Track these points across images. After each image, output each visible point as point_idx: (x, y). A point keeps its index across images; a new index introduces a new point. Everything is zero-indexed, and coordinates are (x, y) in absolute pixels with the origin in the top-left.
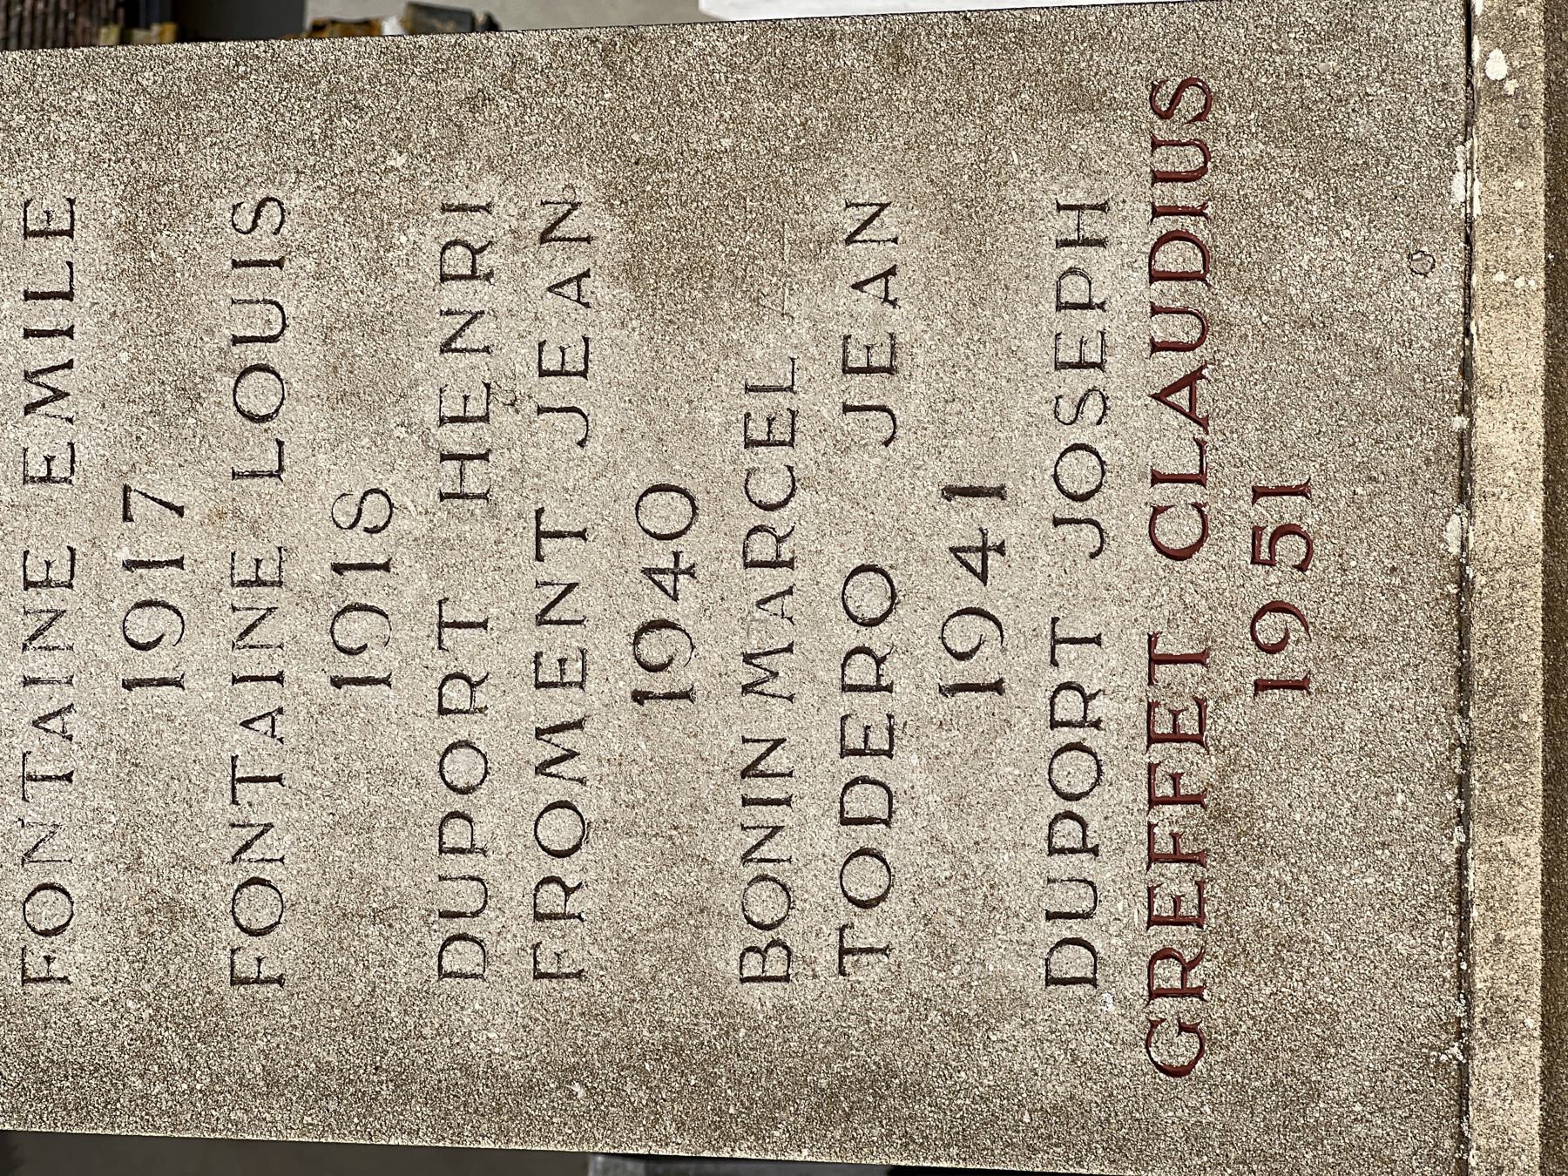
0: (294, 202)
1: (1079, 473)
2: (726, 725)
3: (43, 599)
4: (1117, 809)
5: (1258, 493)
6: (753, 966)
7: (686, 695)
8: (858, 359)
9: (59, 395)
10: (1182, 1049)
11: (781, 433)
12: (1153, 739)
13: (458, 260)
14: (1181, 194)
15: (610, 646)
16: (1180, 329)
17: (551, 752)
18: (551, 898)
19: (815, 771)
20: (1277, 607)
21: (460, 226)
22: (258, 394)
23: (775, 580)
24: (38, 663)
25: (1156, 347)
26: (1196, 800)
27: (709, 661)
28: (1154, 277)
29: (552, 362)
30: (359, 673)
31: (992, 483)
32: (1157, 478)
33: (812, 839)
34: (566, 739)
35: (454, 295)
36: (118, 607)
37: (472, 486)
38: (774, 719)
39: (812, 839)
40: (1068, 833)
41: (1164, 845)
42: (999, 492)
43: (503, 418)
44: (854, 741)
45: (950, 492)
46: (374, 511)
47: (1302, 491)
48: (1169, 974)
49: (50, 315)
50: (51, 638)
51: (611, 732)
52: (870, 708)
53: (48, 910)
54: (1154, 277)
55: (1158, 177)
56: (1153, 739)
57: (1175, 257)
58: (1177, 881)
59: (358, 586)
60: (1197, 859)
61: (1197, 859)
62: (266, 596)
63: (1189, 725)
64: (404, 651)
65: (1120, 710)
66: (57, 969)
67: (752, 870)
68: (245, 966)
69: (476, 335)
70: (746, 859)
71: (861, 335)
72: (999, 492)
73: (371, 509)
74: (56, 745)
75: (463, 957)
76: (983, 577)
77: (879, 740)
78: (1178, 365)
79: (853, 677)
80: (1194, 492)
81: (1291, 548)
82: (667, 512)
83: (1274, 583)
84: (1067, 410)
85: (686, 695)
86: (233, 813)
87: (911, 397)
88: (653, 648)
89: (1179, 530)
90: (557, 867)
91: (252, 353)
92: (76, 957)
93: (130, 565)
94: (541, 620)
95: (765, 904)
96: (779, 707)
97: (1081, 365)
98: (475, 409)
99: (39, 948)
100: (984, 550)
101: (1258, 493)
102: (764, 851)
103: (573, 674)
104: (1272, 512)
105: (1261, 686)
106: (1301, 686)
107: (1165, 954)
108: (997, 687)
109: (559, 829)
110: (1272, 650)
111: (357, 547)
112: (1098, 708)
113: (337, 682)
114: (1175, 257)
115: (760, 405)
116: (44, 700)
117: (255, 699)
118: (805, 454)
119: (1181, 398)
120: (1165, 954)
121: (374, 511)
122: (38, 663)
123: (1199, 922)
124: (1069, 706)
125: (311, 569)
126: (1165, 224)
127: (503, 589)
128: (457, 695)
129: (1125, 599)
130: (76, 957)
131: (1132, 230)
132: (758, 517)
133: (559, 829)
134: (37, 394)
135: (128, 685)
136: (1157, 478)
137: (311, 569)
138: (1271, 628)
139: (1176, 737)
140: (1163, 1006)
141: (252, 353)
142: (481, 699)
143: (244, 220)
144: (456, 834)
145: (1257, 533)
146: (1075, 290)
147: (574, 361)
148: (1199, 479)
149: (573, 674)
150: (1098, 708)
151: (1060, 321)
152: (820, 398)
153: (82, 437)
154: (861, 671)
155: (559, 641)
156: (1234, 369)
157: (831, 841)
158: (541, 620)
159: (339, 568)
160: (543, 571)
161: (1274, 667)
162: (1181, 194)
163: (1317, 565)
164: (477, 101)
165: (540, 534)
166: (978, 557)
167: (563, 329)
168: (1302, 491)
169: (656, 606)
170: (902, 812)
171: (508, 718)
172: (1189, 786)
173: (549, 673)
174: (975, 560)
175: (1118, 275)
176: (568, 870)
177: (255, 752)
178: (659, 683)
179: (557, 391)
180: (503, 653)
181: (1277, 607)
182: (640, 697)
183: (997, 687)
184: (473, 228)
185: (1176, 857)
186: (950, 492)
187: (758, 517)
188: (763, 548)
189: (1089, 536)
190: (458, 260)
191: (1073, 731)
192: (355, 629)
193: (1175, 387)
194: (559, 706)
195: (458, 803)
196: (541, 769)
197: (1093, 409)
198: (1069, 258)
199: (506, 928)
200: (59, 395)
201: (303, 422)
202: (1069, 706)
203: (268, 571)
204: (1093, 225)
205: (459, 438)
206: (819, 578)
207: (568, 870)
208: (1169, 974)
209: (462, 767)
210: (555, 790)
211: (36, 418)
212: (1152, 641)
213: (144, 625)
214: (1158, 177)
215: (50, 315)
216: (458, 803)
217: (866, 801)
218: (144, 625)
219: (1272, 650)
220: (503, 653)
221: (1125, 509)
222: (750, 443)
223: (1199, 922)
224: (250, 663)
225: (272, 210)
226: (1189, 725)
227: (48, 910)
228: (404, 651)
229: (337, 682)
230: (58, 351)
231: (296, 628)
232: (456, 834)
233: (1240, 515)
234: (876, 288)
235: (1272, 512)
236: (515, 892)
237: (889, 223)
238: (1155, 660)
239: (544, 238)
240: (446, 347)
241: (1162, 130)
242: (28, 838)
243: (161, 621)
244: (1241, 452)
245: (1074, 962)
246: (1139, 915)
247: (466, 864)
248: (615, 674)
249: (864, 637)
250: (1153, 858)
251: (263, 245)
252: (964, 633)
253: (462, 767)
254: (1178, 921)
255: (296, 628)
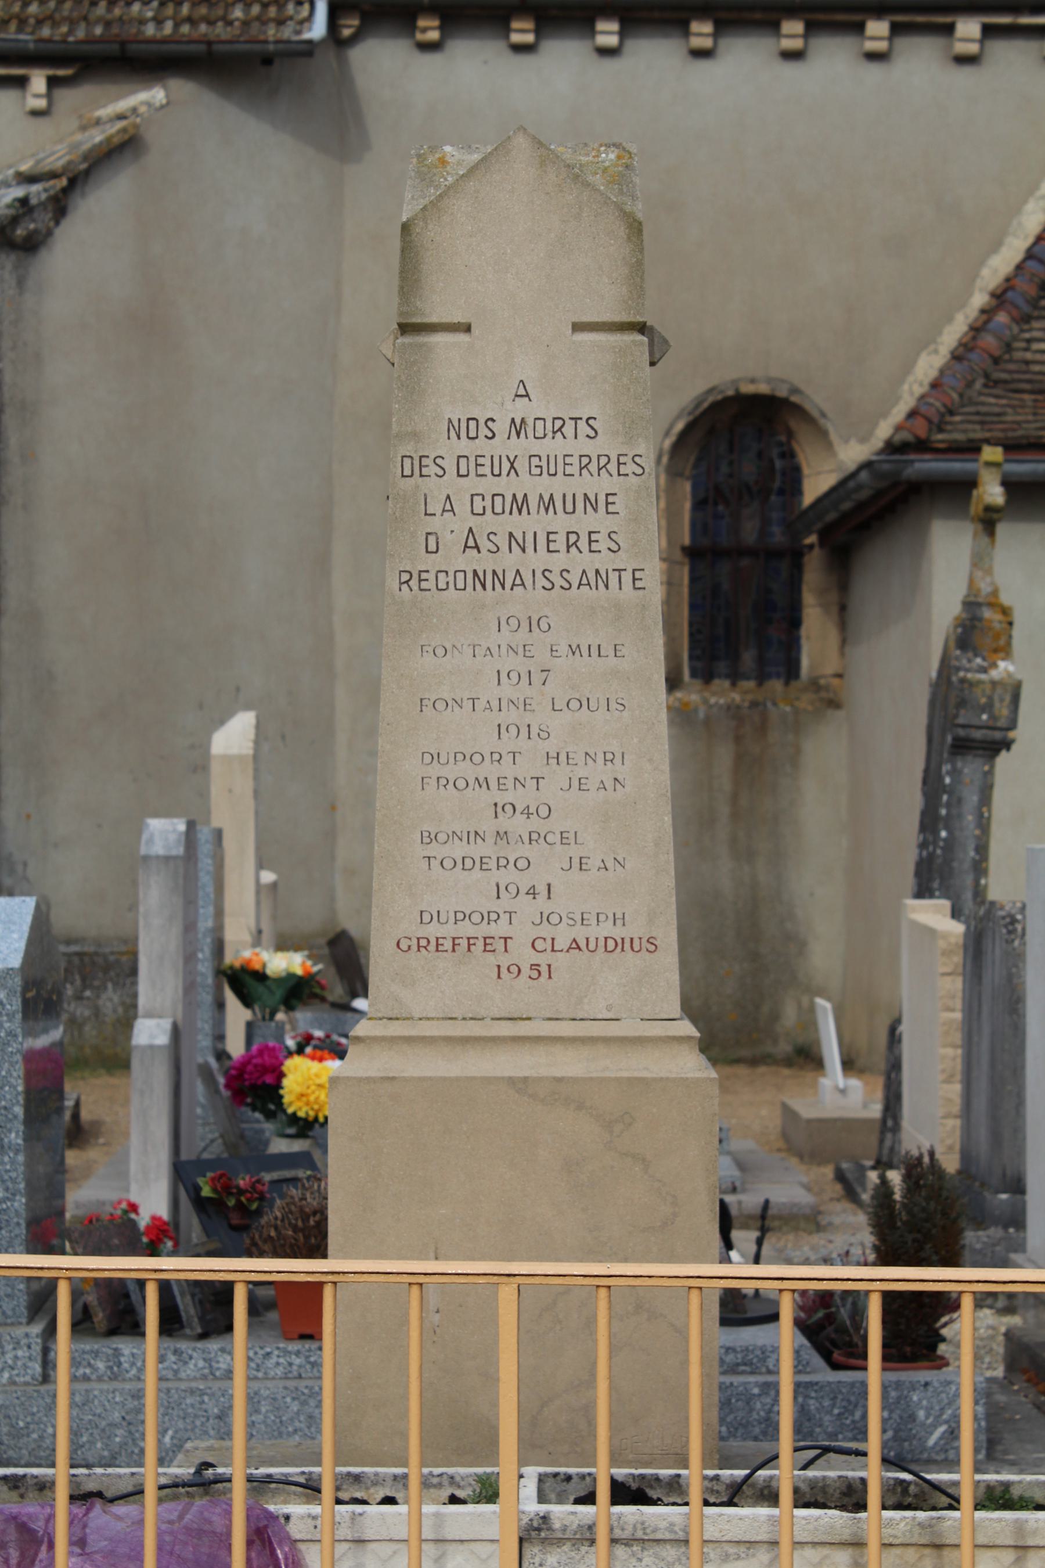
0: (625, 714)
1: (555, 919)
2: (488, 825)
3: (521, 650)
4: (466, 929)
5: (549, 966)
6: (426, 834)
7: (496, 817)
8: (584, 861)
9: (574, 653)
10: (404, 947)
11: (564, 841)
12: (485, 938)
13: (609, 756)
14: (627, 945)
15: (509, 797)
16: (592, 946)
17: (481, 781)
18: (443, 782)
19: (477, 850)
20: (519, 971)
21: (618, 756)
22: (575, 705)
23: (526, 839)
24: (504, 649)
25: (587, 939)
26: (469, 950)
27: (505, 822)
28: (606, 938)
29: (583, 781)
30: (502, 731)
31: (552, 896)
32: (553, 939)
33: (458, 849)
34: (484, 785)
35: (600, 756)
36: (519, 669)
37: (550, 761)
38: (490, 839)
39: (458, 849)
40: (460, 916)
41: (457, 941)
42: (549, 898)
43: (570, 768)
44: (484, 860)
45: (549, 885)
46: (544, 735)
47: (550, 977)
48: (423, 943)
49: (594, 651)
50: (510, 651)
51: (485, 798)
52: (493, 864)
53: (440, 652)
54: (606, 938)
55: (632, 939)
56: (485, 938)
57: (611, 944)
58: (448, 945)
59: (524, 731)
60: (454, 950)
61: (454, 950)
62: (521, 707)
63: (489, 948)
64: (508, 743)
65: (493, 930)
66: (425, 654)
67: (451, 834)
68: (425, 702)
69: (590, 761)
70: (454, 832)
71: (589, 861)
72: (549, 898)
73: (545, 734)
74: (483, 653)
75: (428, 758)
76: (527, 893)
77: (484, 867)
78: (582, 944)
79: (501, 860)
80: (549, 948)
81: (535, 974)
82: (544, 811)
83: (526, 971)
84: (571, 916)
85: (496, 817)
86: (465, 699)
87: (575, 874)
88: (508, 808)
89: (539, 945)
90: (451, 783)
91: (585, 703)
92: (429, 658)
93: (530, 672)
94: (516, 779)
95: (442, 837)
96: (493, 840)
97: (583, 919)
98: (571, 761)
99: (431, 650)
100: (534, 894)
101: (549, 966)
102: (456, 838)
103: (501, 787)
104: (544, 969)
105: (499, 967)
106: (499, 977)
107: (429, 942)
108: (498, 897)
109: (461, 784)
110: (508, 969)
111: (534, 731)
112: (493, 923)
113: (499, 726)
114: (611, 944)
115: (572, 836)
116: (495, 650)
117: (495, 704)
118: (558, 847)
119: (574, 945)
120: (429, 942)
121: (544, 735)
122: (504, 649)
123: (437, 950)
124: (493, 916)
125: (528, 718)
126: (619, 941)
127: (525, 769)
128: (496, 757)
129: (522, 932)
130: (429, 658)
131: (618, 932)
132: (542, 835)
133: (461, 784)
134: (574, 648)
135: (498, 672)
136: (553, 939)
137: (528, 718)
138: (514, 969)
139: (485, 944)
140: (415, 941)
141: (585, 703)
142: (496, 763)
143: (619, 701)
144: (460, 757)
145: (538, 965)
146: (602, 918)
147: (583, 787)
148: (553, 950)
149: (501, 787)
150: (493, 923)
151: (594, 914)
152: (575, 851)
153: (564, 658)
154: (503, 862)
155: (510, 783)
156: (580, 958)
157: (458, 856)
158: (516, 779)
159: (529, 726)
160: (528, 779)
161: (504, 970)
162: (627, 945)
163: (531, 981)
164: (650, 760)
165: (538, 778)
166: (532, 892)
167: (593, 784)
168: (550, 977)
169: (519, 808)
170: (466, 873)
171: (489, 770)
172: (472, 948)
173: (502, 781)
174: (532, 891)
175: (607, 929)
176: (451, 786)
177: (480, 705)
178: (499, 809)
179: (575, 783)
180: (507, 769)
181: (519, 971)
182: (496, 805)
183: (498, 897)
184: (618, 760)
185: (454, 945)
186: (549, 885)
187: (542, 835)
188: (534, 836)
189: (538, 921)
190: (609, 756)
191: (488, 917)
192: (513, 730)
193: (577, 944)
194: (493, 784)
195: (468, 757)
196: (477, 779)
197: (571, 922)
198: (611, 916)
199: (435, 770)
200: (574, 653)
201: (566, 716)
202: (493, 916)
203: (528, 707)
204: (619, 922)
205: (563, 758)
206: (525, 850)
207: (451, 786)
208: (423, 943)
209: (477, 758)
210: (471, 782)
211: (567, 647)
212: (511, 938)
213: (514, 676)
214: (632, 939)
215: (594, 651)
216: (468, 757)
217: (468, 863)
218: (514, 676)
219: (508, 969)
220: (507, 769)
221: (546, 931)
222: (562, 833)
223: (437, 950)
224: (504, 704)
225: (622, 708)
226: (489, 948)
227: (440, 652)
228: (508, 743)
229: (499, 726)
230: (585, 653)
231: (511, 716)
232: (460, 757)
233: (543, 960)
234: (602, 866)
235: (544, 969)
236: (444, 772)
237: (619, 868)
238: (506, 939)
239: (616, 779)
240: (587, 754)
241: (644, 941)
242: (459, 646)
243: (515, 679)
244: (560, 961)
245: (426, 918)
246: (439, 935)
247: (452, 760)
248: (501, 798)
249: (512, 862)
250: (454, 939)
251: (613, 705)
252: (513, 889)
253: (477, 758)
254: (437, 945)
255: (511, 716)
